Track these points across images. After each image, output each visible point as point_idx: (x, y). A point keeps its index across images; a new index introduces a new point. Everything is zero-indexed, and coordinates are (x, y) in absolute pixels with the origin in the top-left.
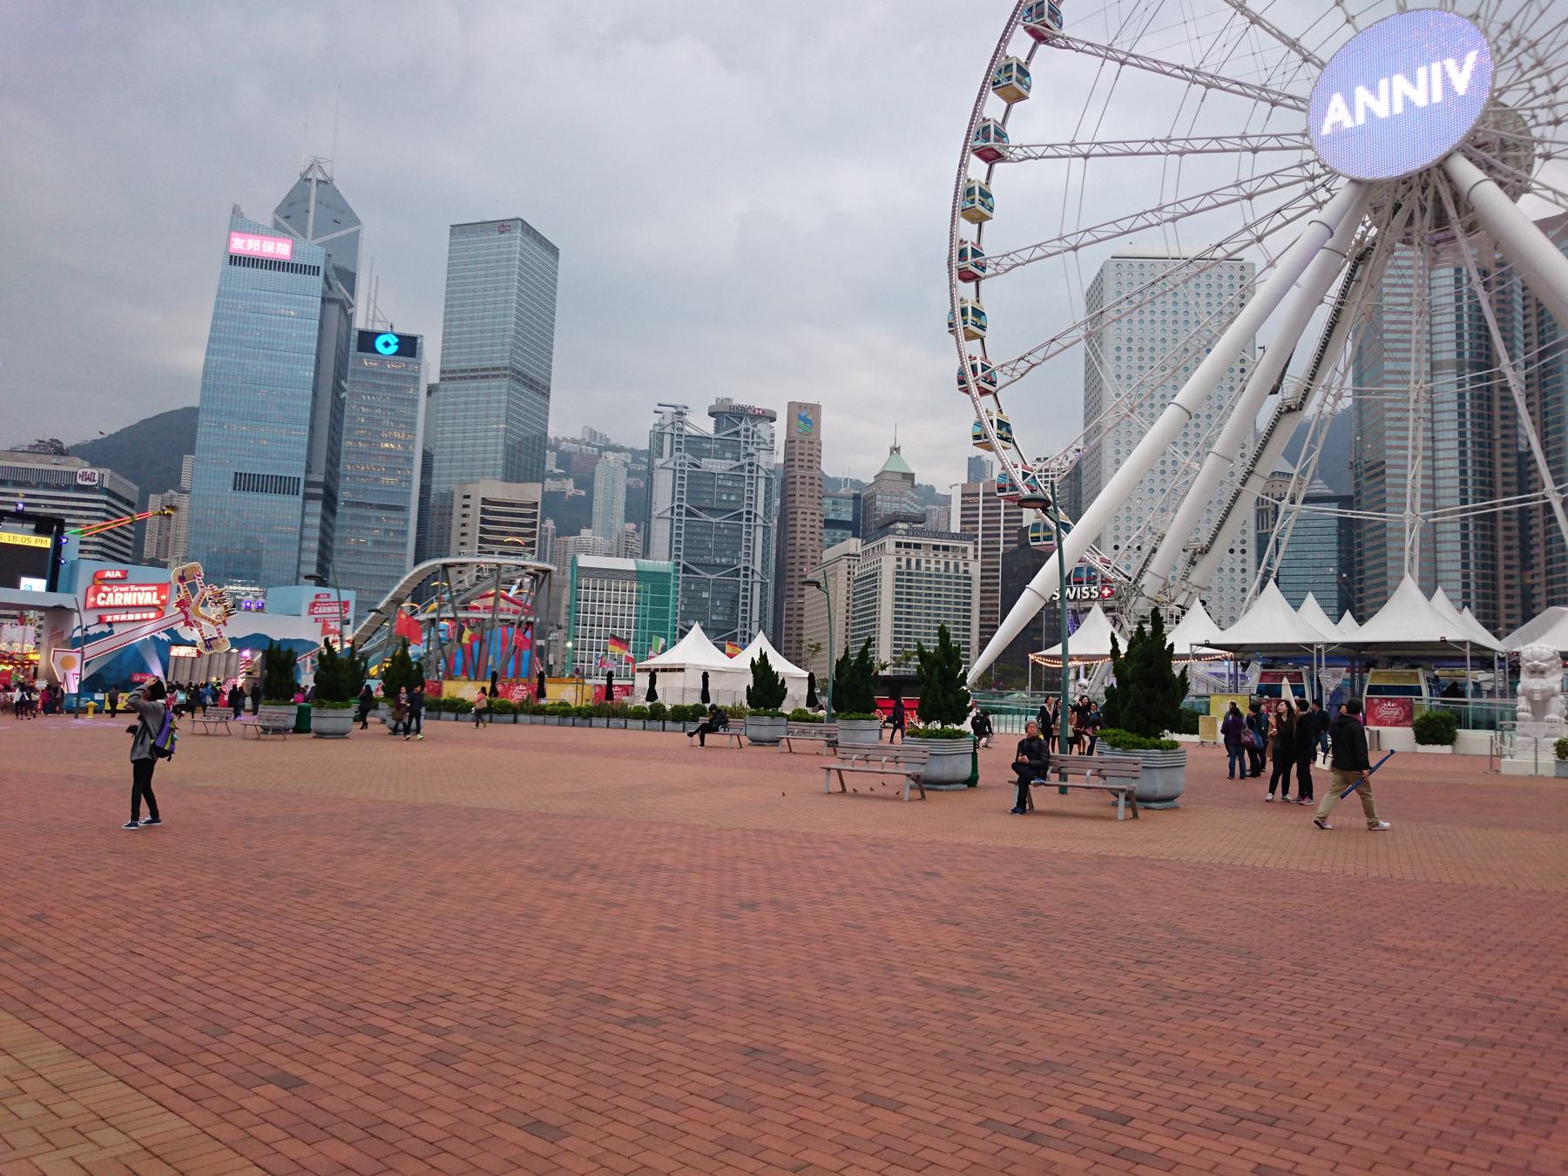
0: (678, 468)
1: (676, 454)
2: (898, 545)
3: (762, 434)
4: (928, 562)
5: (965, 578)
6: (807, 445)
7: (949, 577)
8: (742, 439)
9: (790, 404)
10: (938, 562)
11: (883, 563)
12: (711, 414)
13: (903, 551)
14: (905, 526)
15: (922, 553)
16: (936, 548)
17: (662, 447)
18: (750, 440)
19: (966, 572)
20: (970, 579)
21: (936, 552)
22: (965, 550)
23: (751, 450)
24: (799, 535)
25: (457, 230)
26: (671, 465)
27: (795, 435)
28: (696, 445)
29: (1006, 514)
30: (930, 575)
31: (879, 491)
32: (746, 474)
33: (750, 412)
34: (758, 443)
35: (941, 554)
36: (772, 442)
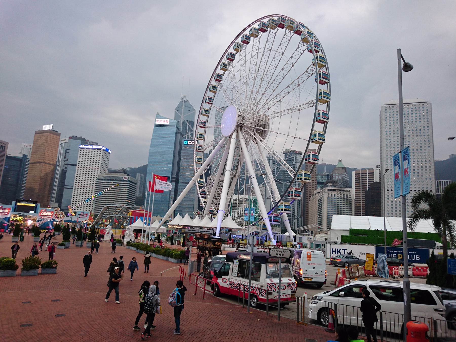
2: (328, 190)
3: (297, 158)
4: (338, 194)
5: (350, 199)
7: (348, 199)
8: (292, 160)
10: (341, 195)
11: (324, 195)
13: (330, 192)
14: (331, 184)
15: (336, 192)
16: (340, 190)
18: (294, 160)
19: (350, 197)
20: (351, 199)
21: (340, 192)
22: (350, 191)
23: (294, 163)
24: (309, 187)
29: (369, 179)
30: (338, 199)
33: (294, 152)
34: (297, 161)
35: (342, 192)
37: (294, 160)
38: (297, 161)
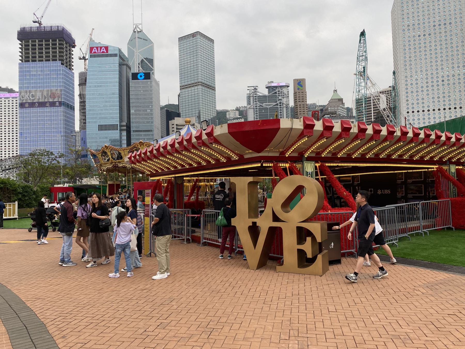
0: (255, 108)
1: (255, 103)
3: (284, 92)
6: (301, 94)
8: (277, 95)
9: (294, 80)
12: (267, 88)
17: (250, 102)
18: (280, 95)
23: (280, 98)
25: (181, 39)
26: (252, 107)
27: (297, 91)
28: (263, 99)
31: (329, 107)
32: (279, 107)
34: (283, 95)
36: (288, 94)
37: (280, 95)
38: (283, 95)
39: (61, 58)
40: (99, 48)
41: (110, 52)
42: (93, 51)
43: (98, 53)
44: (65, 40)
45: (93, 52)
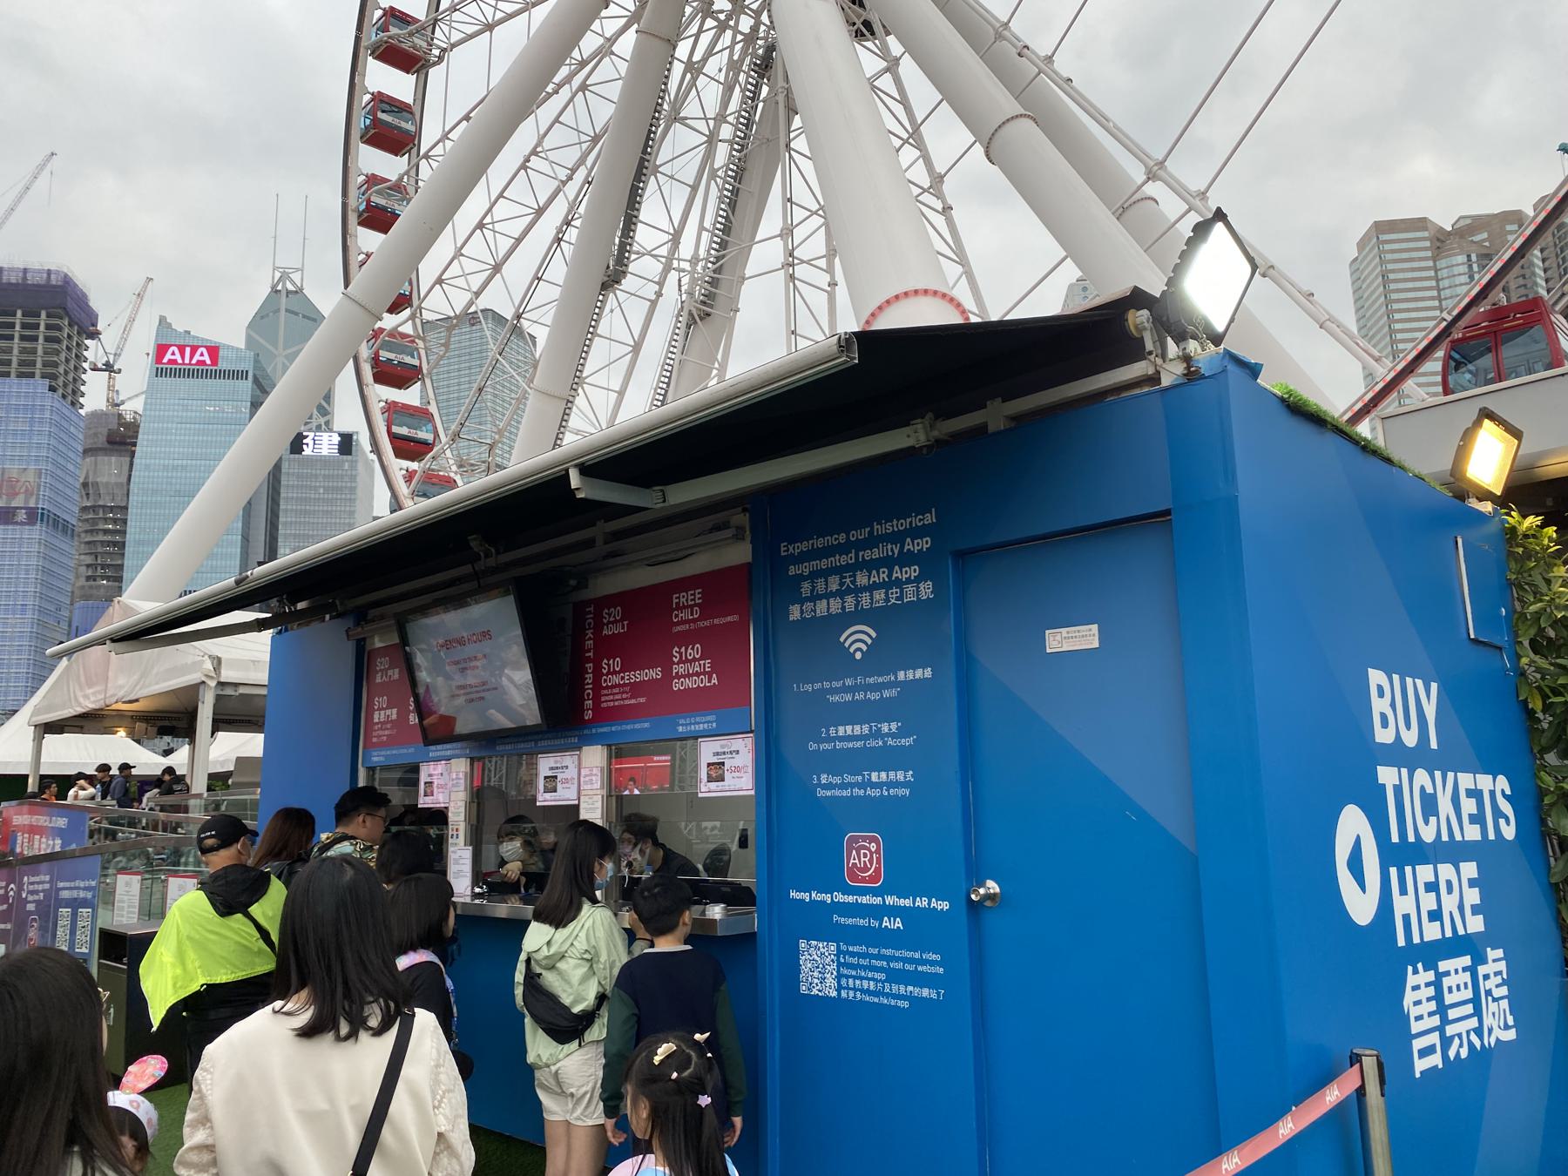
39: (49, 370)
40: (188, 350)
41: (223, 365)
42: (168, 356)
43: (184, 364)
44: (67, 314)
45: (165, 360)
